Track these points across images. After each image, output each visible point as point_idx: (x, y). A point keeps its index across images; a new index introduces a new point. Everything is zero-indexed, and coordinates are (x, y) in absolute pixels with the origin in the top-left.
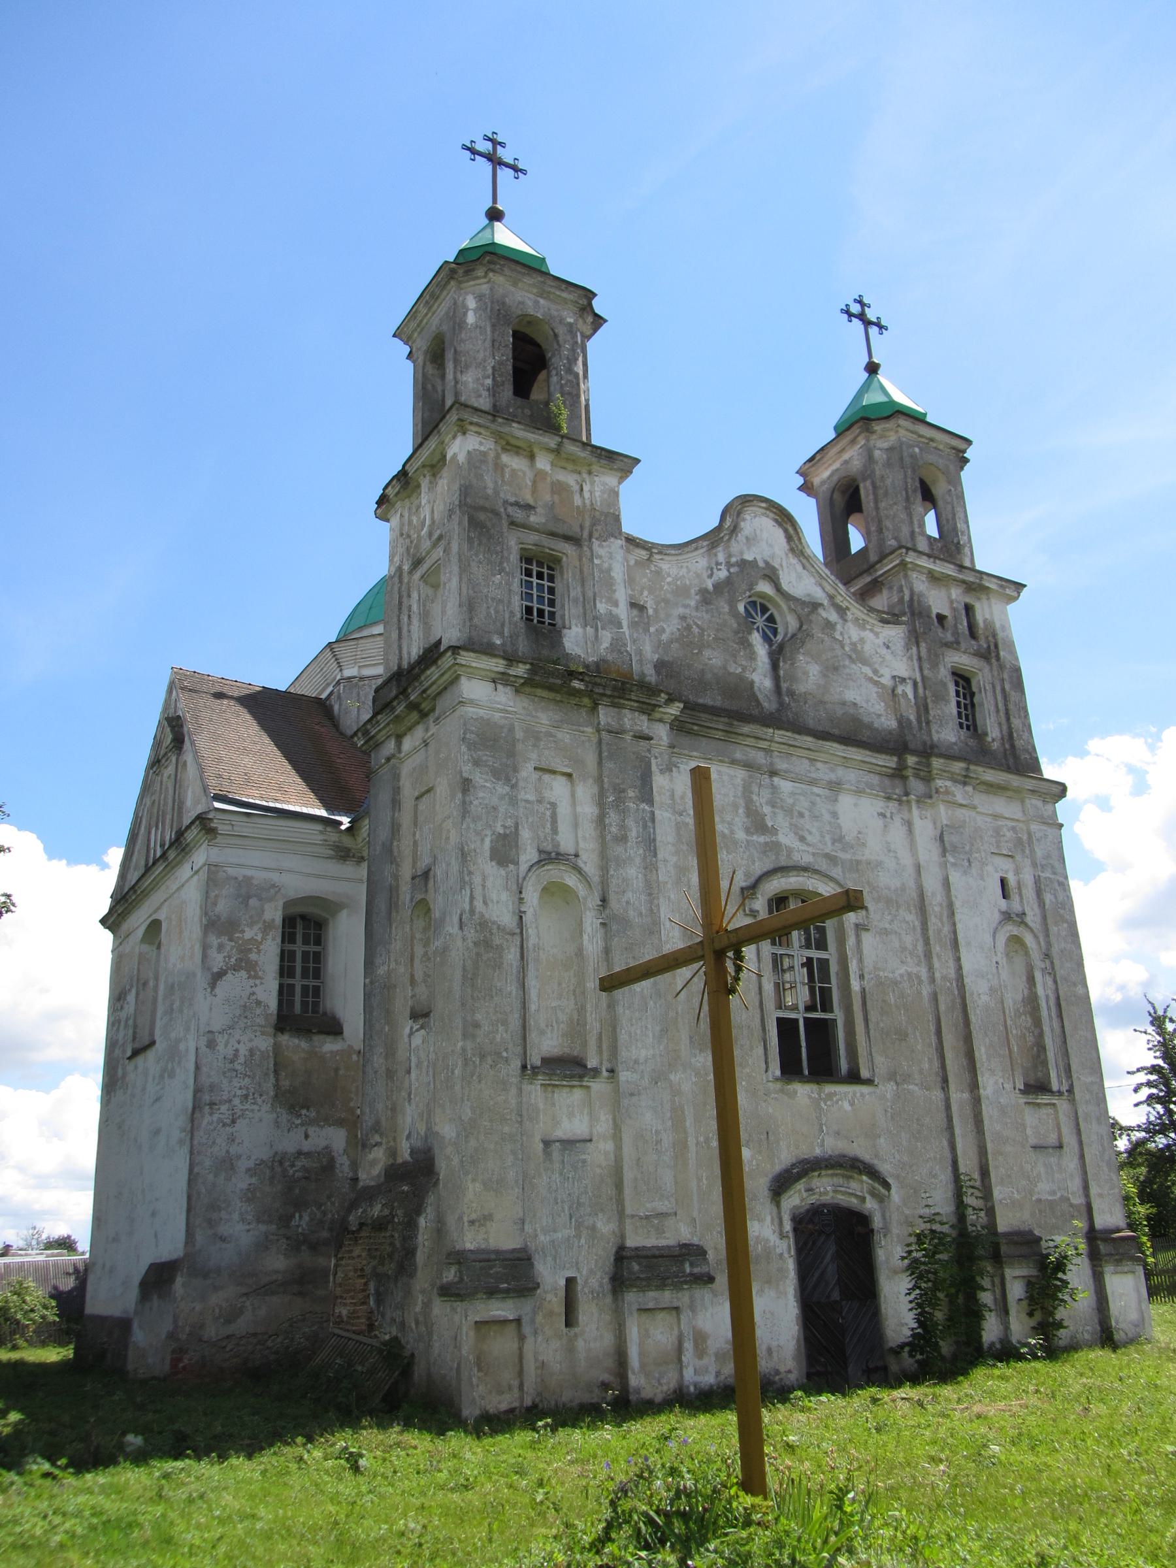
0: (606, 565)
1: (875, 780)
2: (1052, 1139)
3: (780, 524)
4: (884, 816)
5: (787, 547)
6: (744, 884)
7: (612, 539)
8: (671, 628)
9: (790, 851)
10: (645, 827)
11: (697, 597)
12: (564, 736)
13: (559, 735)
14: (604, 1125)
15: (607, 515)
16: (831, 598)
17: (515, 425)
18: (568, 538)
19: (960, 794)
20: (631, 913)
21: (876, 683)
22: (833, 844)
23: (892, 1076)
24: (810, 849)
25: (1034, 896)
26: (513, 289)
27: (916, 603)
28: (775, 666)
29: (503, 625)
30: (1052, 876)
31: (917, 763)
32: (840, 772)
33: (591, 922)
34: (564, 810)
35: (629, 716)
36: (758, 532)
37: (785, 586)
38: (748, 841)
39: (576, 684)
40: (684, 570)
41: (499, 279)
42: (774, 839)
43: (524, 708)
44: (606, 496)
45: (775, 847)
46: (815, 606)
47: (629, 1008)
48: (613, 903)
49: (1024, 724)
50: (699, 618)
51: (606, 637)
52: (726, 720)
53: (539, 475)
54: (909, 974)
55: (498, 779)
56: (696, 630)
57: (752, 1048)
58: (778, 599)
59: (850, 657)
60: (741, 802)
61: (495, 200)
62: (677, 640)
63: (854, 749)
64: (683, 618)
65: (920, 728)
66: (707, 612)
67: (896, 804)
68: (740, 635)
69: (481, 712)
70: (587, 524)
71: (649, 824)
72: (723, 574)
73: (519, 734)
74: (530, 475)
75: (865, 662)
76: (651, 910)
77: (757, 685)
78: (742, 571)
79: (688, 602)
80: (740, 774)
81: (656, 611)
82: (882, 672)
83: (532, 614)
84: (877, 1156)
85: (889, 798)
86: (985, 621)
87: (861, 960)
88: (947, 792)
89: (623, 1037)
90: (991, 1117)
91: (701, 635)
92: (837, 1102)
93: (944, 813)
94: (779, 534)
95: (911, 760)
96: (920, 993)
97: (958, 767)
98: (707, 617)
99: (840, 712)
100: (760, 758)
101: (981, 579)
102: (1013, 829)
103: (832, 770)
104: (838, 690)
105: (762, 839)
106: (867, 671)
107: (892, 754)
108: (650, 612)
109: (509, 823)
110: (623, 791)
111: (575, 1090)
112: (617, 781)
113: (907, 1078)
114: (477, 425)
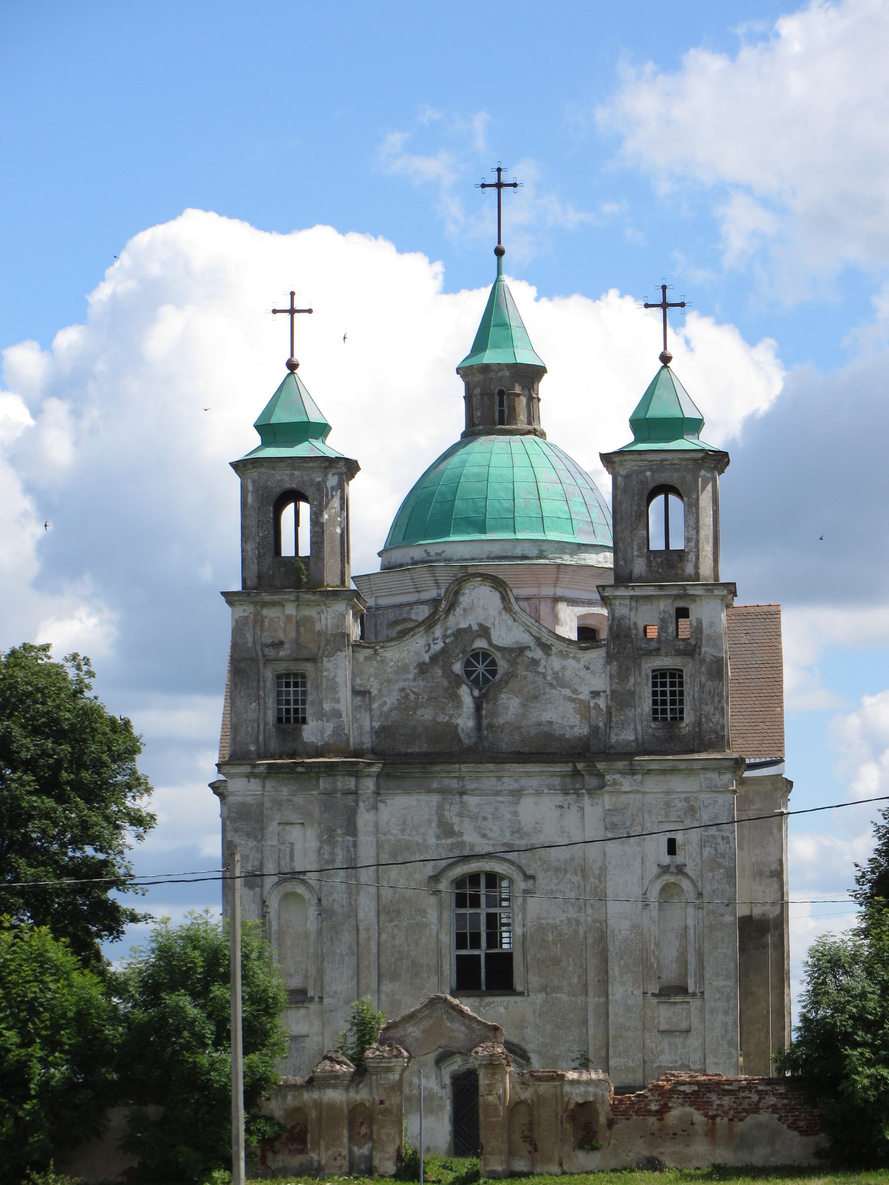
0: (332, 675)
1: (557, 781)
2: (684, 1026)
3: (496, 589)
4: (561, 807)
5: (502, 606)
6: (431, 874)
7: (339, 653)
8: (392, 699)
9: (472, 846)
10: (348, 851)
11: (416, 671)
12: (299, 799)
13: (296, 799)
14: (316, 1027)
15: (335, 636)
16: (538, 640)
17: (263, 594)
18: (307, 660)
19: (627, 783)
20: (336, 906)
21: (574, 700)
22: (512, 835)
23: (544, 989)
24: (491, 842)
25: (698, 850)
26: (273, 472)
27: (615, 627)
28: (478, 708)
29: (258, 736)
30: (716, 834)
31: (585, 767)
32: (524, 782)
33: (312, 912)
34: (298, 848)
35: (341, 780)
36: (475, 602)
37: (495, 641)
38: (437, 845)
39: (300, 769)
40: (406, 652)
41: (263, 470)
42: (460, 839)
43: (272, 787)
44: (336, 621)
45: (462, 844)
46: (521, 650)
47: (331, 963)
48: (324, 903)
49: (716, 708)
50: (415, 687)
51: (329, 727)
52: (420, 766)
53: (289, 618)
54: (569, 920)
55: (250, 838)
56: (412, 696)
57: (429, 978)
58: (493, 650)
59: (551, 685)
60: (435, 818)
61: (292, 355)
62: (396, 708)
63: (531, 765)
64: (402, 690)
65: (606, 732)
66: (423, 680)
67: (574, 796)
68: (450, 691)
69: (239, 799)
70: (323, 644)
71: (352, 849)
72: (440, 645)
73: (268, 804)
74: (283, 618)
75: (564, 685)
76: (350, 903)
77: (461, 726)
78: (456, 639)
79: (407, 676)
80: (435, 798)
81: (380, 690)
82: (580, 690)
83: (290, 714)
84: (523, 1039)
85: (566, 794)
86: (697, 619)
87: (524, 915)
88: (615, 783)
89: (327, 979)
90: (617, 1014)
91: (416, 699)
92: (494, 1007)
93: (607, 801)
94: (496, 596)
95: (580, 766)
96: (576, 932)
97: (621, 765)
98: (421, 683)
99: (533, 731)
100: (454, 784)
101: (685, 590)
102: (687, 800)
103: (516, 781)
104: (535, 714)
105: (449, 841)
106: (568, 692)
107: (567, 762)
108: (374, 692)
109: (256, 863)
110: (334, 830)
111: (300, 1009)
112: (330, 825)
113: (558, 989)
114: (238, 601)
